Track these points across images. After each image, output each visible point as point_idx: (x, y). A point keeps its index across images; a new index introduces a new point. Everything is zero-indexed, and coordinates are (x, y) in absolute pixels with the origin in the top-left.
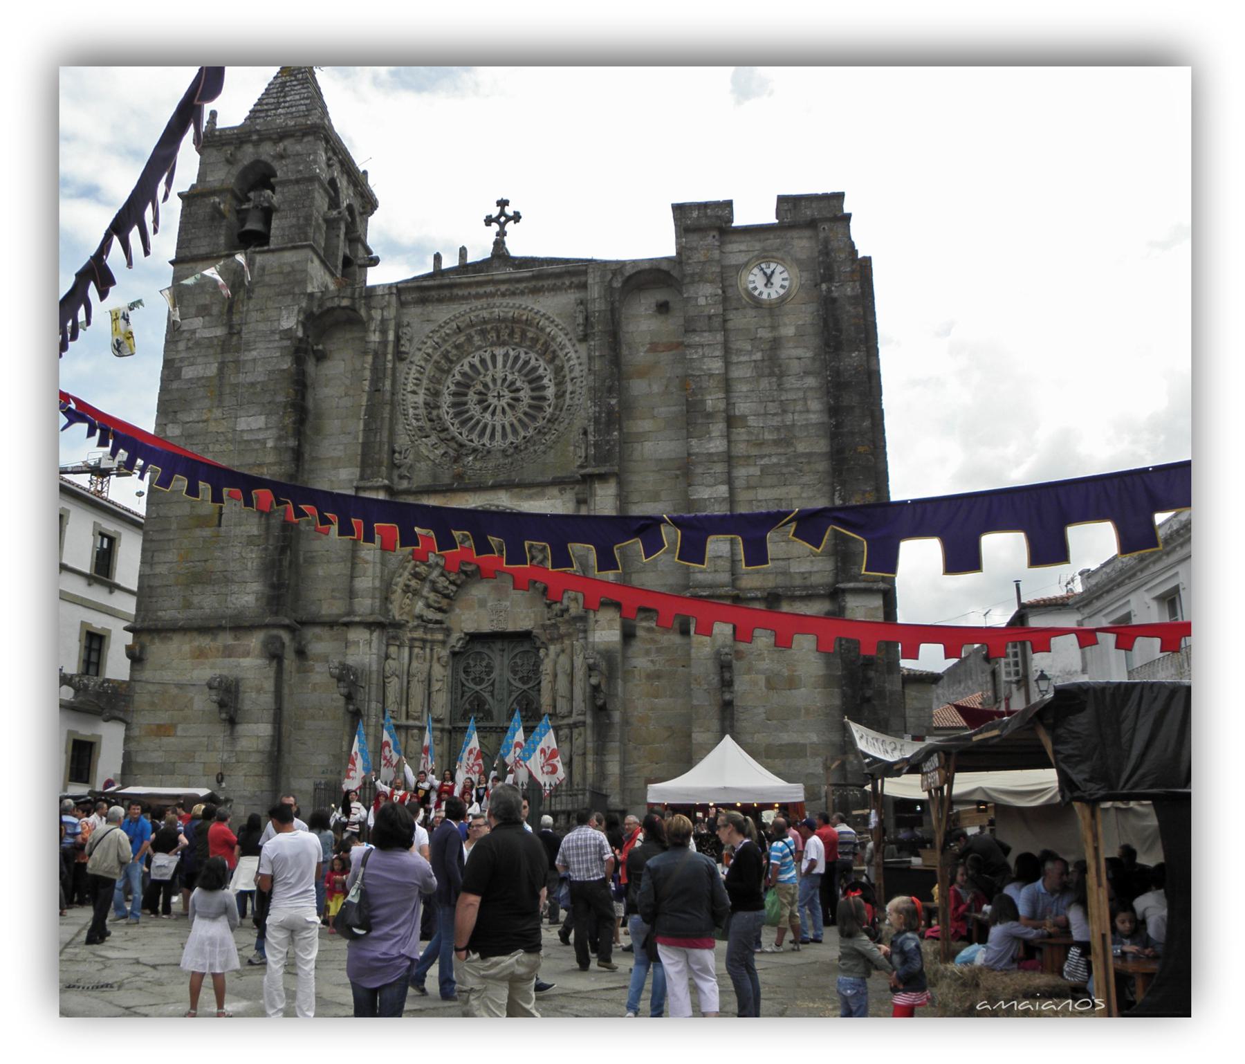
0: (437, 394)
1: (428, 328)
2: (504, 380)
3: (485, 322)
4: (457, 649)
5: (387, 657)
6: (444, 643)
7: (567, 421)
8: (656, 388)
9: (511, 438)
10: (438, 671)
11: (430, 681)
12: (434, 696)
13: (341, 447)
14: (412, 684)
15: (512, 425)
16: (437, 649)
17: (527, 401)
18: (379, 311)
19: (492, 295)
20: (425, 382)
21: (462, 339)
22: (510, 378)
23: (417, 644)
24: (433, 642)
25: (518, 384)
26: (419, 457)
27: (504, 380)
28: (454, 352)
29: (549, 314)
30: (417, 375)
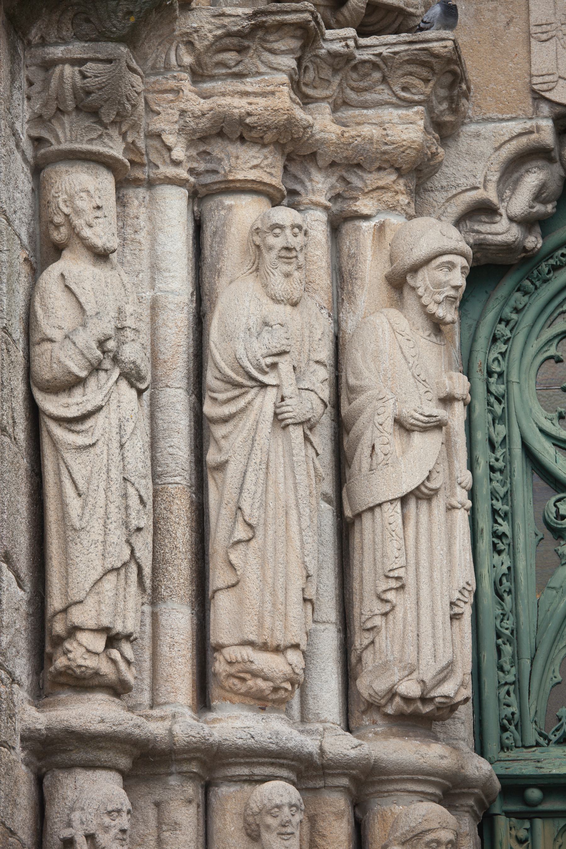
4: (502, 231)
5: (47, 249)
6: (418, 173)
10: (406, 364)
11: (341, 428)
12: (385, 540)
14: (229, 445)
16: (381, 210)
23: (251, 163)
24: (350, 164)
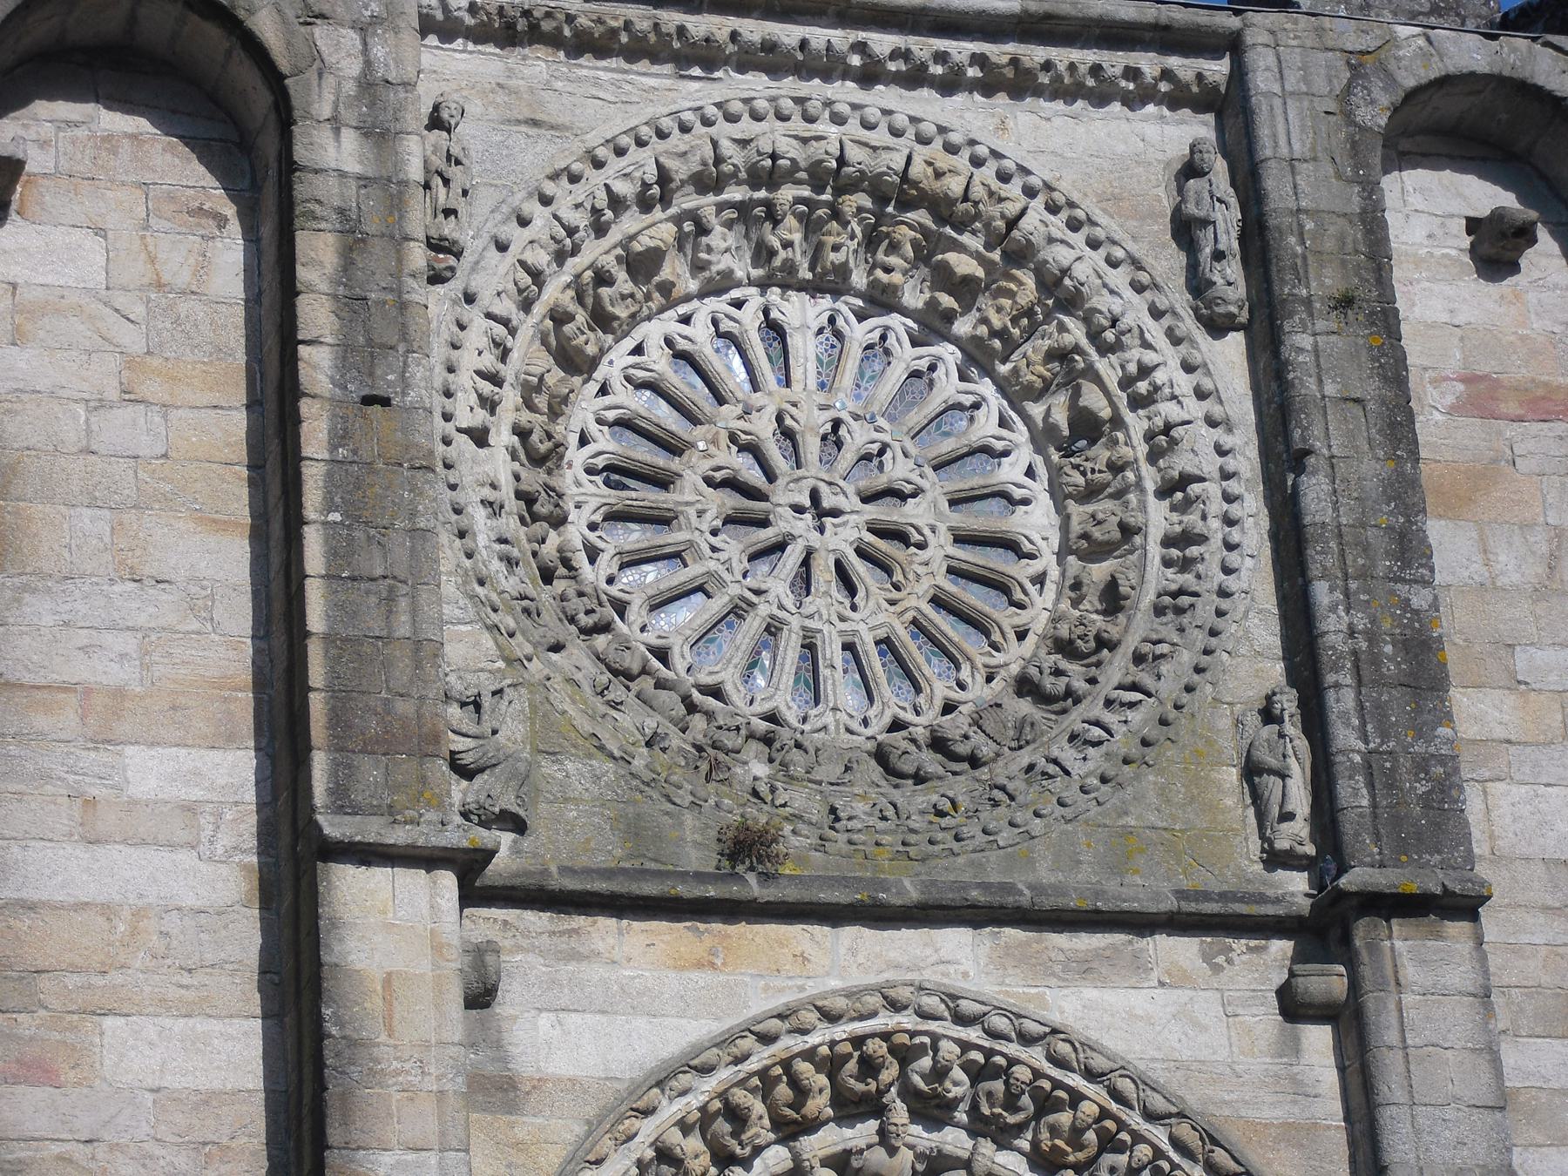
0: (545, 458)
1: (535, 156)
2: (833, 437)
3: (768, 175)
7: (1186, 657)
8: (1514, 564)
9: (893, 700)
13: (128, 643)
15: (887, 645)
17: (941, 548)
18: (351, 38)
19: (828, 67)
20: (510, 397)
21: (658, 230)
22: (858, 437)
25: (897, 470)
26: (550, 738)
27: (833, 437)
28: (623, 282)
29: (1067, 187)
30: (489, 361)
